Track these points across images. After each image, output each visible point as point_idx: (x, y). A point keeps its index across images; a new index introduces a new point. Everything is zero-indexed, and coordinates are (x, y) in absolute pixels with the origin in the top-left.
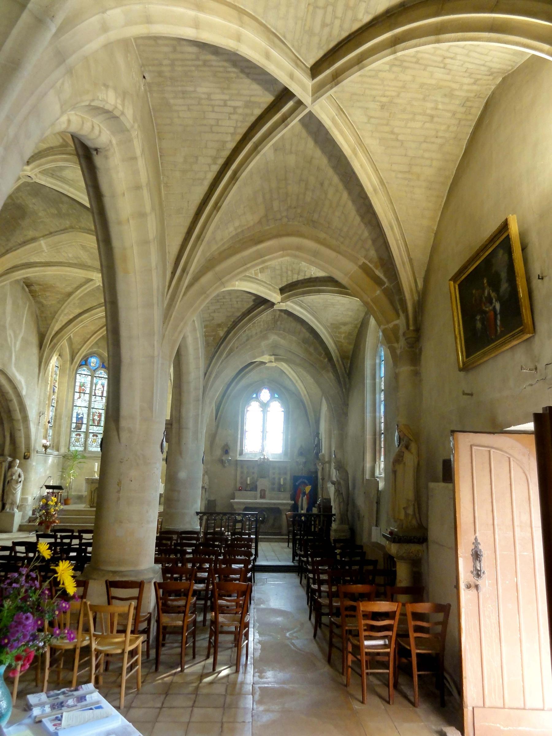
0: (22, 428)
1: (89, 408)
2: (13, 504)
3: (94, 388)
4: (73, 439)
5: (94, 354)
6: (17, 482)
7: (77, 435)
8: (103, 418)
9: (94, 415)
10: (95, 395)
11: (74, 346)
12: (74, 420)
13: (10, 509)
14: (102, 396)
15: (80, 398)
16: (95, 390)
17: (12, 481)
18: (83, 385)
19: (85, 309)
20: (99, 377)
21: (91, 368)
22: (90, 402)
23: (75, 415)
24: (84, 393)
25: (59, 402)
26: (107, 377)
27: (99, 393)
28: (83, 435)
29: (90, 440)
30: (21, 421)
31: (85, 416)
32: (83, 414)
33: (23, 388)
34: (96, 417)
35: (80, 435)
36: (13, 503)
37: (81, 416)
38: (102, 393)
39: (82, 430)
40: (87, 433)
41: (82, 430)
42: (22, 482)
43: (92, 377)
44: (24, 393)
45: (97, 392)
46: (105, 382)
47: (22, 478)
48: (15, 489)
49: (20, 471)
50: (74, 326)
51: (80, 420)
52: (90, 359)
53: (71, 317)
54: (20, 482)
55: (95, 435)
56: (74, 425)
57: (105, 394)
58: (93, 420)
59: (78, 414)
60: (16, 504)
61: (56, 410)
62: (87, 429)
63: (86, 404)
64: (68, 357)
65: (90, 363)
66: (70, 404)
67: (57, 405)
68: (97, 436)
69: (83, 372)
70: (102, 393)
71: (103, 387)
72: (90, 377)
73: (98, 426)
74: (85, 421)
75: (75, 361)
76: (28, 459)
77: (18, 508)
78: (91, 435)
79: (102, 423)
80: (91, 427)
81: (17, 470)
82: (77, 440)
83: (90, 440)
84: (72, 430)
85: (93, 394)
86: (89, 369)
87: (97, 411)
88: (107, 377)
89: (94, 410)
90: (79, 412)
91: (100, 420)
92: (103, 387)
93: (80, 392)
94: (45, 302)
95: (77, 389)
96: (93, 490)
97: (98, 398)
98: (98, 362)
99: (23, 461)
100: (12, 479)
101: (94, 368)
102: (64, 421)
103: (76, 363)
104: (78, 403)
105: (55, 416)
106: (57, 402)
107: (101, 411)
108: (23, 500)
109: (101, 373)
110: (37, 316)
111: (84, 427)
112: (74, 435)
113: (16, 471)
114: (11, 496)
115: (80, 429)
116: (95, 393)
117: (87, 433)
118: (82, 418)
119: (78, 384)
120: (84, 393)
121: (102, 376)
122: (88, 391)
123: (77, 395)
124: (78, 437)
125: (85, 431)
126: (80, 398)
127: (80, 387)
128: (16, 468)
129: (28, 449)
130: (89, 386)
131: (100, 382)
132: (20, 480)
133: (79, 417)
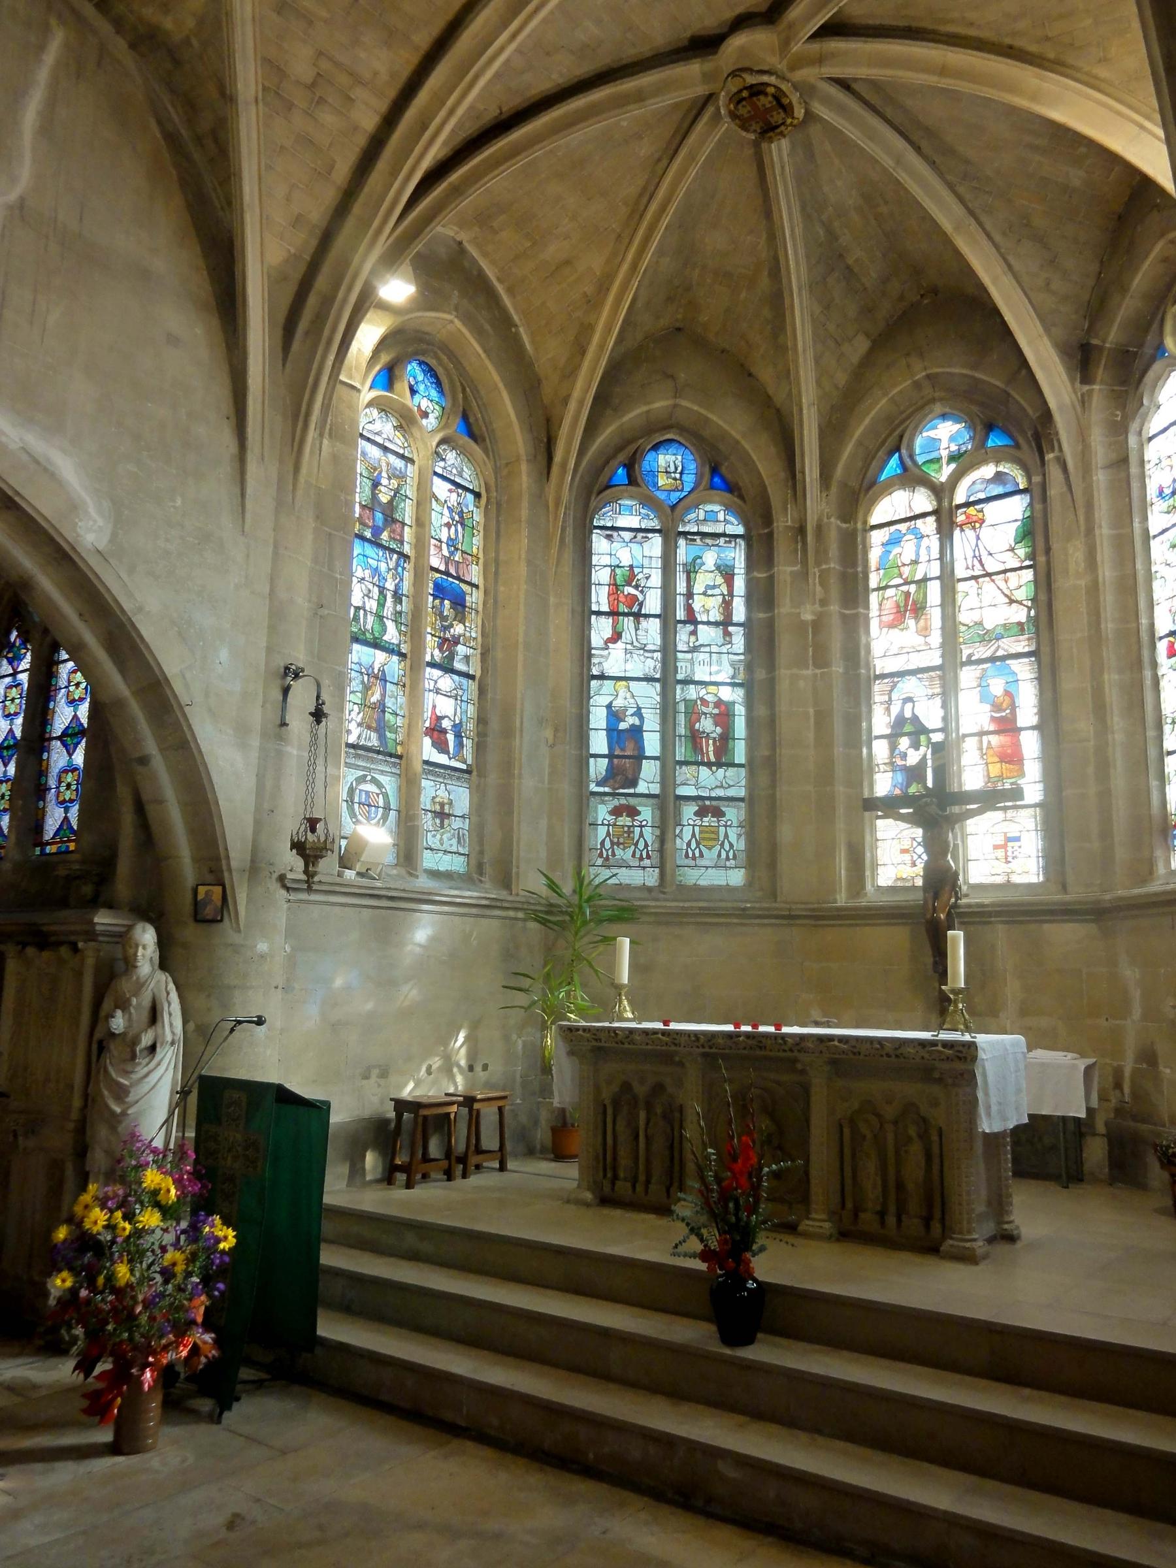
0: (151, 747)
1: (667, 678)
3: (681, 587)
4: (602, 832)
5: (667, 428)
7: (616, 812)
8: (740, 727)
9: (693, 712)
10: (691, 619)
11: (547, 391)
12: (599, 743)
14: (726, 622)
15: (616, 636)
16: (689, 595)
17: (114, 1048)
18: (630, 579)
19: (424, 39)
20: (704, 535)
21: (662, 496)
22: (668, 649)
23: (598, 718)
24: (638, 616)
25: (499, 654)
26: (740, 530)
27: (708, 606)
28: (647, 813)
29: (687, 835)
30: (136, 709)
31: (652, 722)
32: (638, 713)
33: (74, 507)
34: (706, 725)
35: (633, 812)
37: (632, 720)
38: (727, 605)
39: (642, 788)
40: (667, 804)
41: (642, 788)
43: (670, 536)
44: (90, 532)
45: (697, 604)
46: (737, 556)
48: (121, 1093)
50: (394, 173)
51: (625, 739)
52: (650, 456)
53: (369, 122)
54: (153, 1049)
55: (709, 808)
56: (598, 767)
57: (739, 612)
58: (695, 738)
59: (614, 715)
61: (482, 691)
62: (667, 779)
63: (650, 665)
64: (516, 438)
65: (654, 474)
66: (563, 665)
67: (484, 670)
68: (718, 813)
69: (622, 522)
70: (727, 605)
71: (729, 577)
72: (657, 541)
73: (719, 765)
74: (652, 744)
75: (558, 458)
76: (216, 921)
78: (689, 811)
79: (740, 753)
80: (685, 772)
82: (623, 838)
83: (687, 835)
84: (593, 788)
85: (681, 614)
86: (649, 502)
87: (709, 694)
88: (740, 530)
89: (692, 692)
90: (619, 703)
91: (726, 738)
92: (729, 577)
93: (613, 613)
94: (168, 24)
95: (600, 599)
96: (606, 1095)
97: (707, 634)
98: (692, 467)
99: (189, 932)
101: (675, 497)
102: (533, 742)
103: (564, 465)
104: (614, 661)
105: (482, 720)
106: (485, 653)
107: (726, 694)
109: (711, 518)
110: (171, 138)
111: (649, 772)
112: (602, 812)
114: (103, 1132)
115: (634, 783)
116: (690, 610)
117: (667, 804)
118: (636, 732)
119: (601, 576)
120: (638, 616)
121: (719, 529)
122: (653, 603)
123: (601, 629)
124: (624, 820)
125: (655, 789)
126: (616, 636)
127: (615, 587)
129: (214, 866)
130: (656, 579)
131: (710, 558)
133: (623, 726)
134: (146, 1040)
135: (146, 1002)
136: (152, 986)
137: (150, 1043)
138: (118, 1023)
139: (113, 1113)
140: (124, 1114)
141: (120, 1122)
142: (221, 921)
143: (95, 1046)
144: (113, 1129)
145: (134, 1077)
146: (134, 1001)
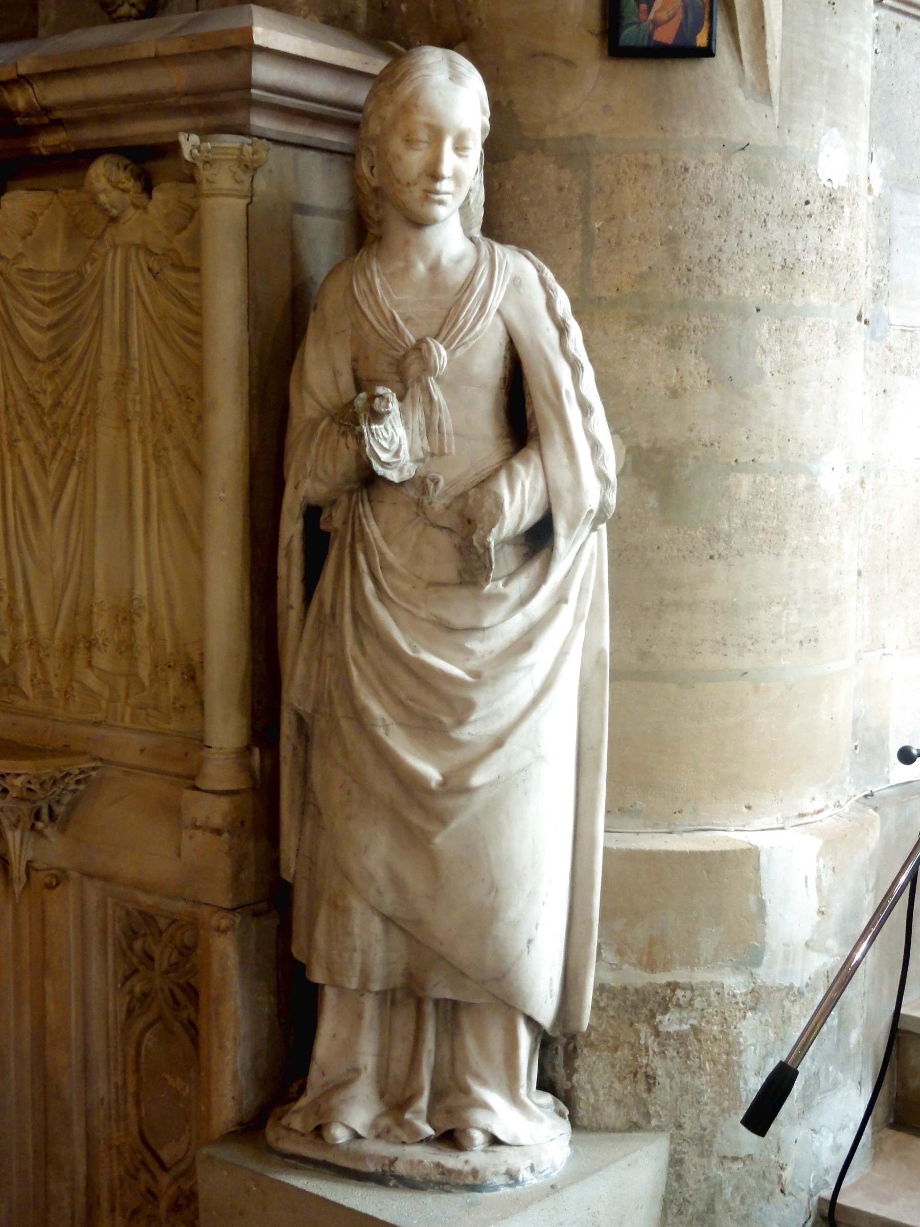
2: (451, 1012)
6: (469, 553)
13: (396, 1103)
17: (384, 533)
36: (444, 997)
42: (582, 553)
47: (588, 455)
48: (438, 708)
49: (521, 291)
54: (539, 538)
60: (508, 1006)
76: (689, 51)
77: (558, 1065)
81: (477, 281)
99: (592, 97)
100: (368, 480)
108: (661, 904)
113: (450, 306)
114: (374, 850)
128: (451, 236)
132: (517, 501)
134: (517, 501)
135: (488, 363)
136: (495, 301)
137: (530, 517)
138: (394, 442)
139: (411, 783)
140: (456, 785)
141: (442, 819)
142: (708, 52)
143: (291, 529)
144: (416, 840)
145: (483, 647)
146: (441, 355)
